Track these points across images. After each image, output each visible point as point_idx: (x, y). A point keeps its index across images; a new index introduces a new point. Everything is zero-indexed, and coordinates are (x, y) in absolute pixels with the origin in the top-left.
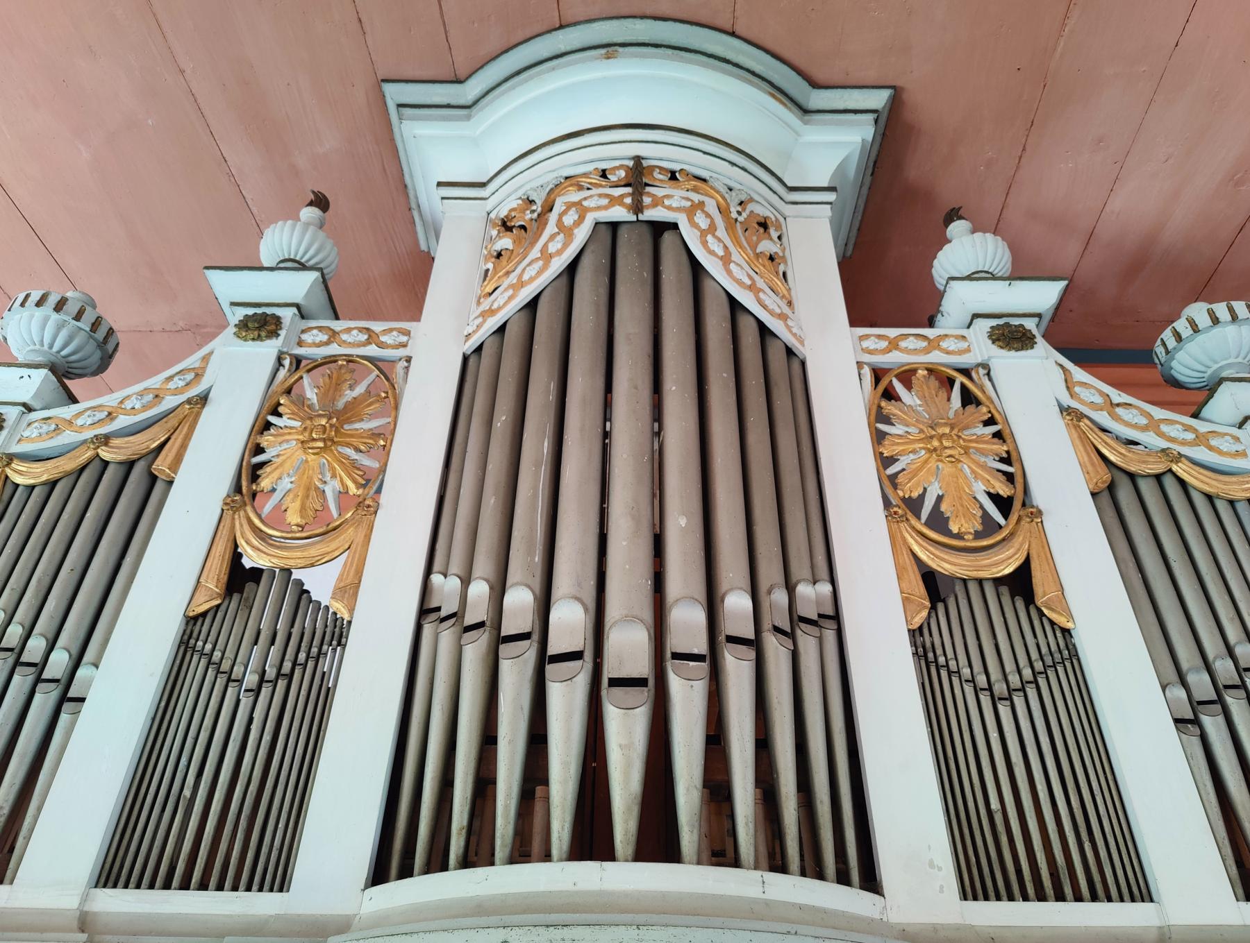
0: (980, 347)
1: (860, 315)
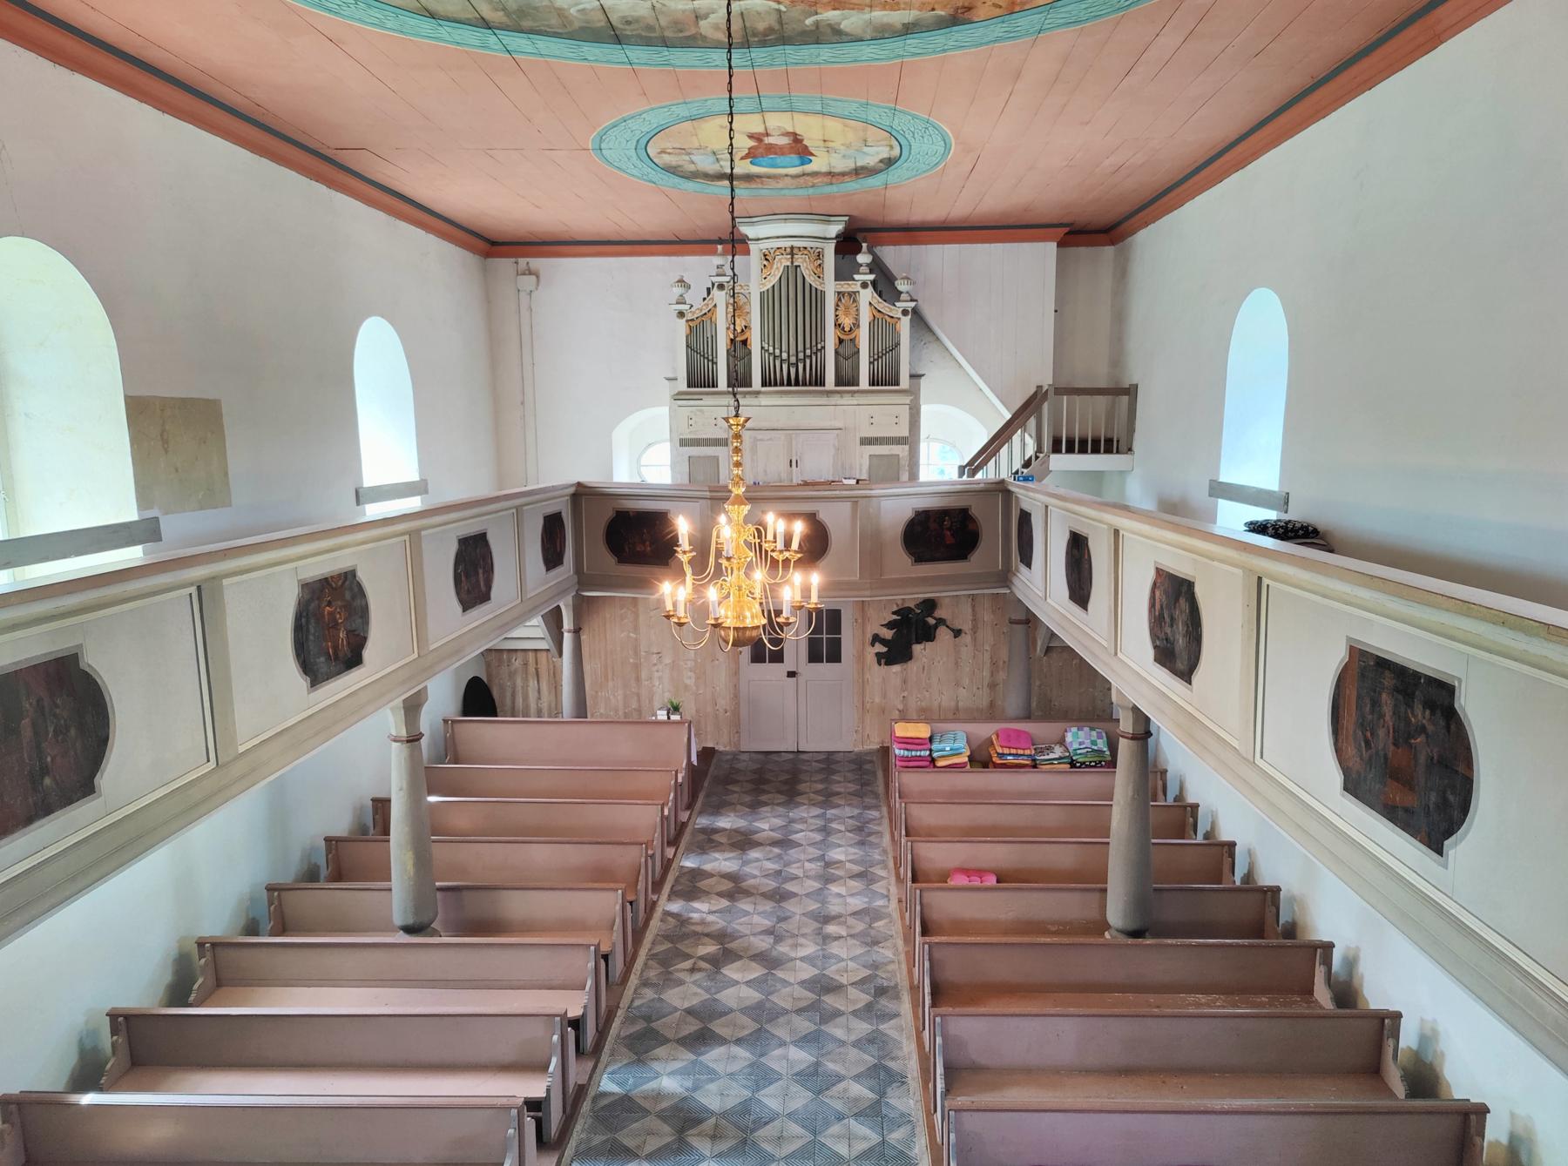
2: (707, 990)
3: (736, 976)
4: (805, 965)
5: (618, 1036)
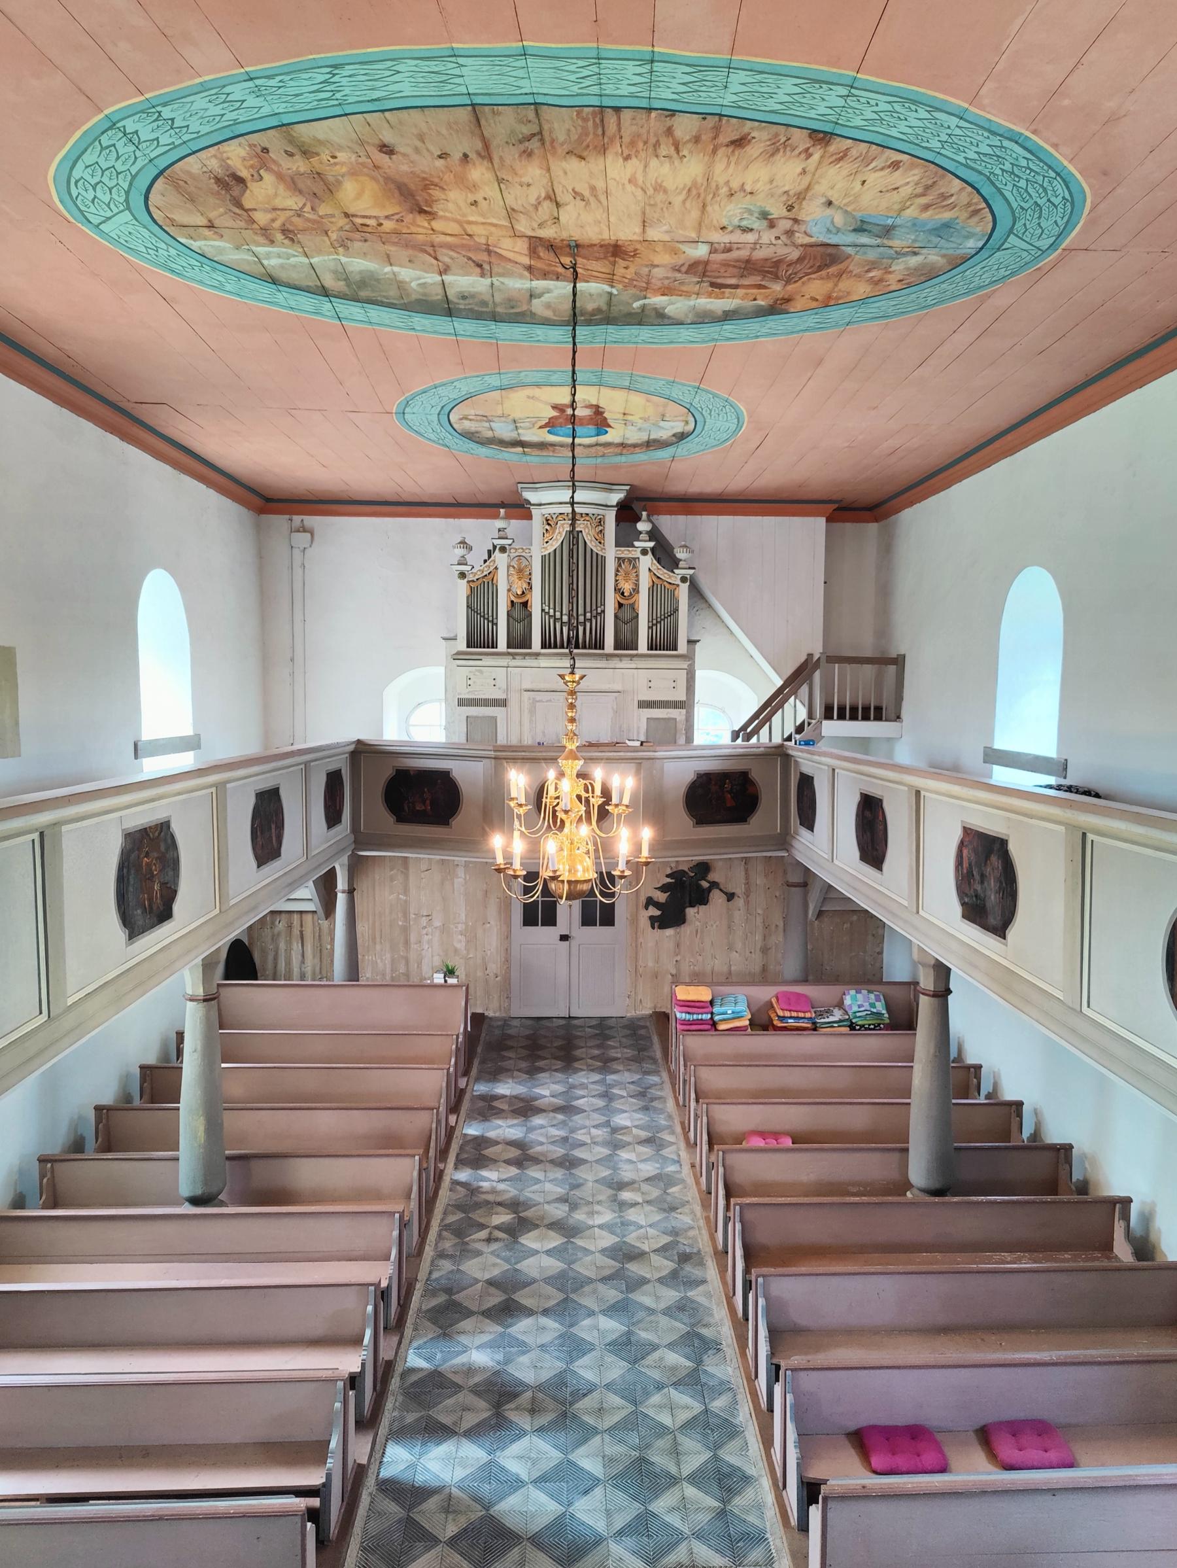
0: (637, 554)
2: (507, 1260)
3: (535, 1246)
4: (604, 1233)
5: (419, 1310)
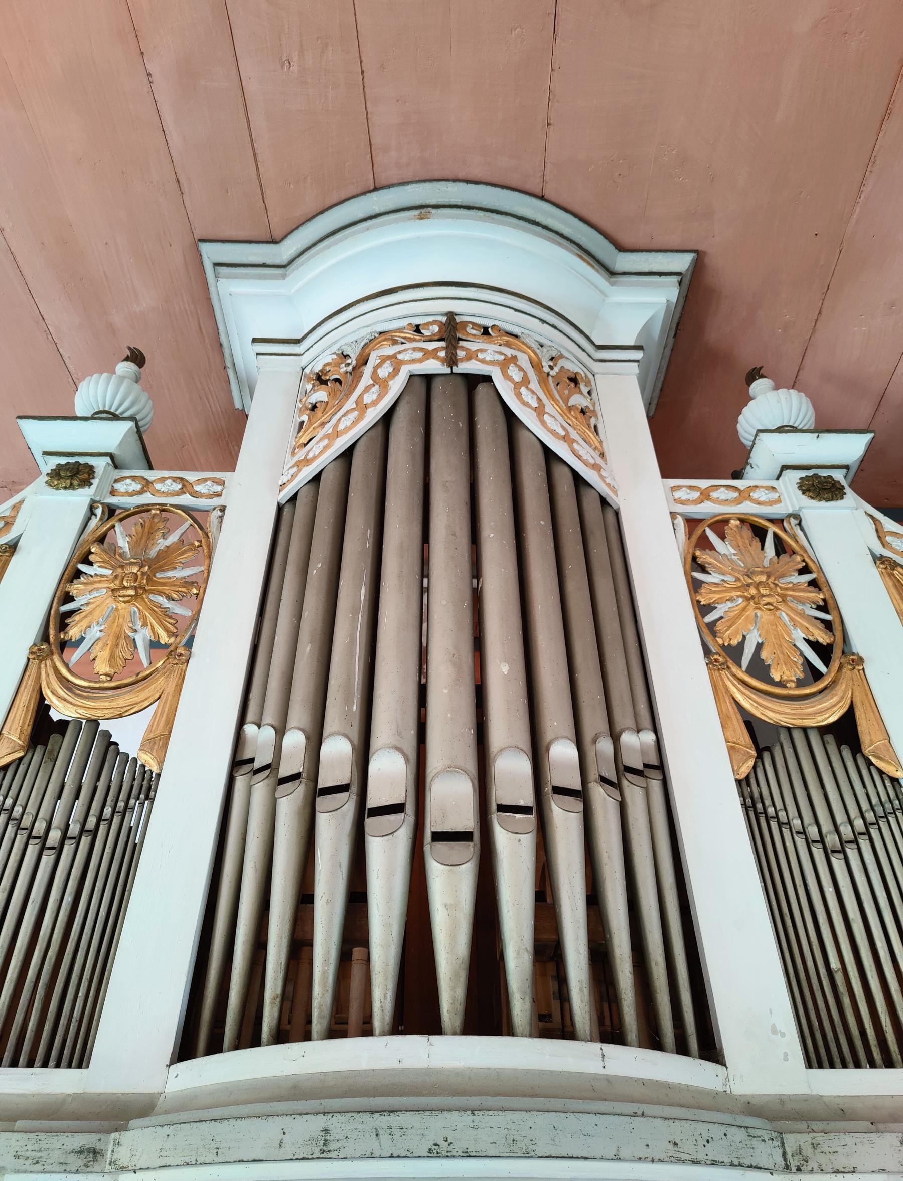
0: (790, 497)
1: (671, 465)
